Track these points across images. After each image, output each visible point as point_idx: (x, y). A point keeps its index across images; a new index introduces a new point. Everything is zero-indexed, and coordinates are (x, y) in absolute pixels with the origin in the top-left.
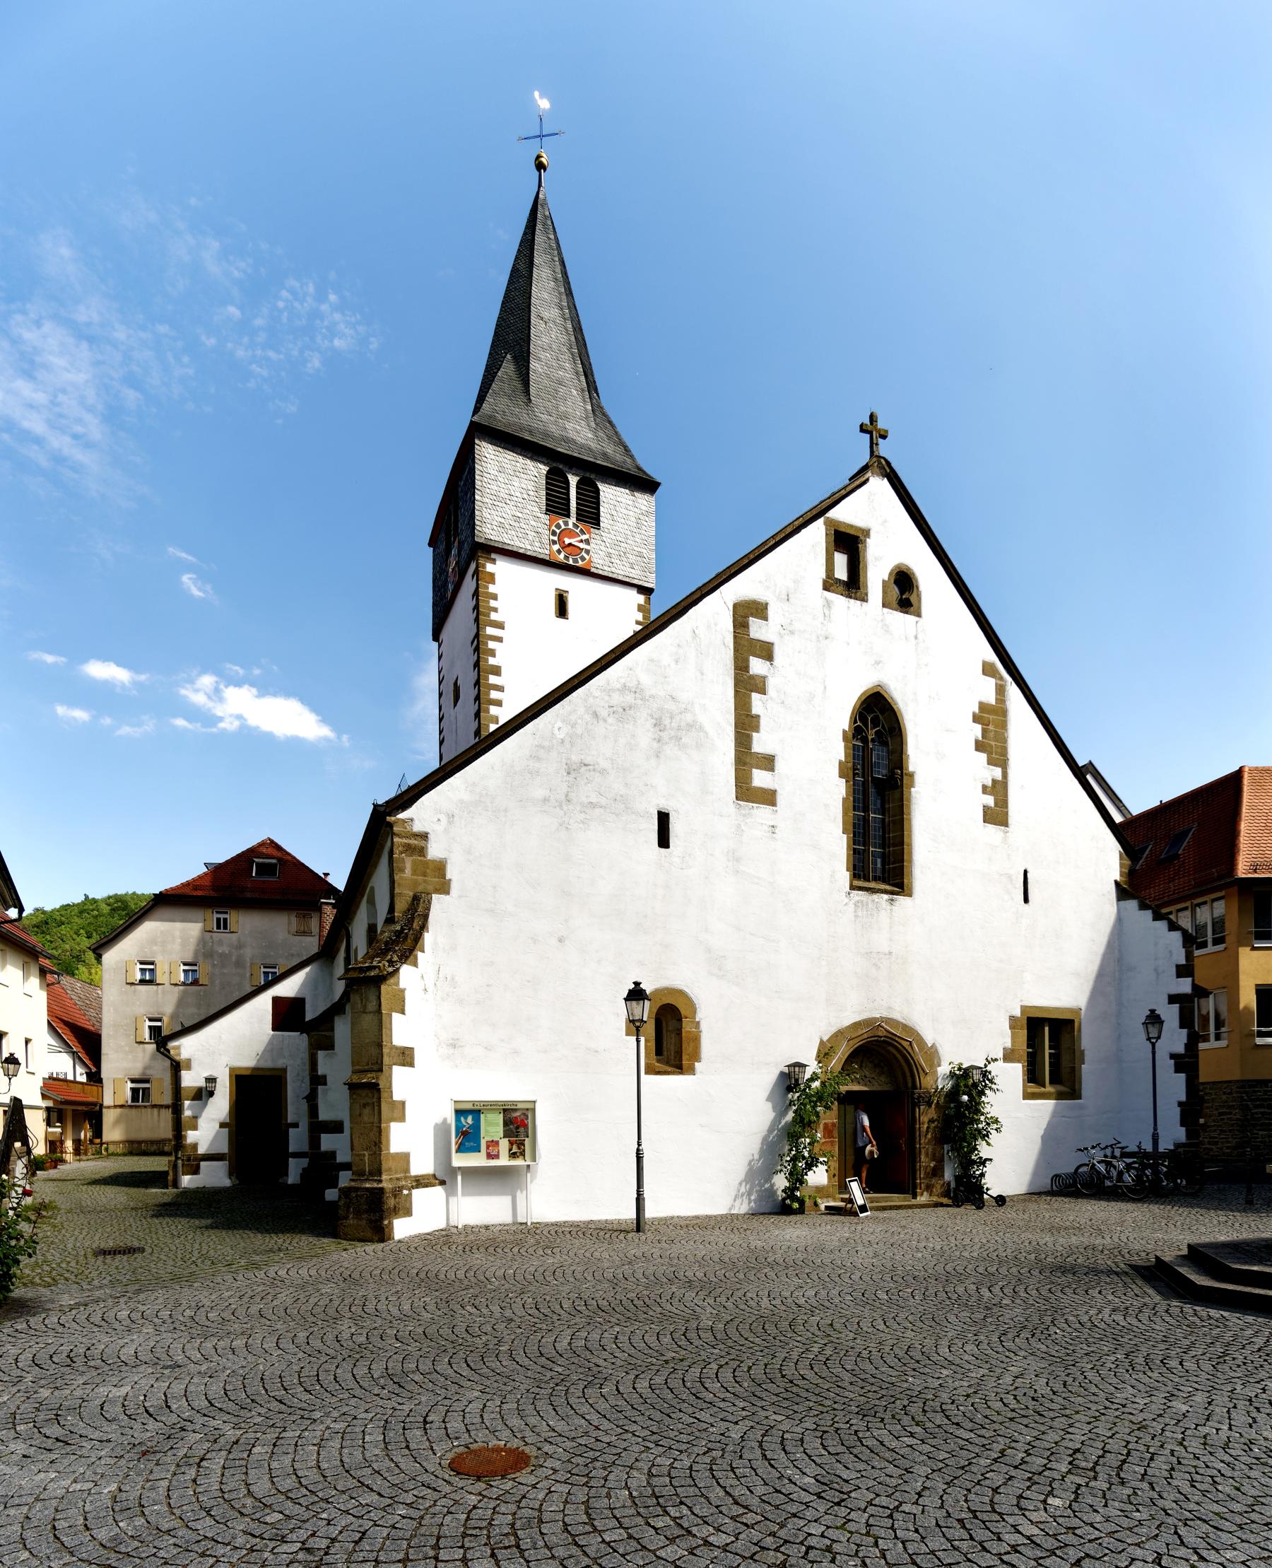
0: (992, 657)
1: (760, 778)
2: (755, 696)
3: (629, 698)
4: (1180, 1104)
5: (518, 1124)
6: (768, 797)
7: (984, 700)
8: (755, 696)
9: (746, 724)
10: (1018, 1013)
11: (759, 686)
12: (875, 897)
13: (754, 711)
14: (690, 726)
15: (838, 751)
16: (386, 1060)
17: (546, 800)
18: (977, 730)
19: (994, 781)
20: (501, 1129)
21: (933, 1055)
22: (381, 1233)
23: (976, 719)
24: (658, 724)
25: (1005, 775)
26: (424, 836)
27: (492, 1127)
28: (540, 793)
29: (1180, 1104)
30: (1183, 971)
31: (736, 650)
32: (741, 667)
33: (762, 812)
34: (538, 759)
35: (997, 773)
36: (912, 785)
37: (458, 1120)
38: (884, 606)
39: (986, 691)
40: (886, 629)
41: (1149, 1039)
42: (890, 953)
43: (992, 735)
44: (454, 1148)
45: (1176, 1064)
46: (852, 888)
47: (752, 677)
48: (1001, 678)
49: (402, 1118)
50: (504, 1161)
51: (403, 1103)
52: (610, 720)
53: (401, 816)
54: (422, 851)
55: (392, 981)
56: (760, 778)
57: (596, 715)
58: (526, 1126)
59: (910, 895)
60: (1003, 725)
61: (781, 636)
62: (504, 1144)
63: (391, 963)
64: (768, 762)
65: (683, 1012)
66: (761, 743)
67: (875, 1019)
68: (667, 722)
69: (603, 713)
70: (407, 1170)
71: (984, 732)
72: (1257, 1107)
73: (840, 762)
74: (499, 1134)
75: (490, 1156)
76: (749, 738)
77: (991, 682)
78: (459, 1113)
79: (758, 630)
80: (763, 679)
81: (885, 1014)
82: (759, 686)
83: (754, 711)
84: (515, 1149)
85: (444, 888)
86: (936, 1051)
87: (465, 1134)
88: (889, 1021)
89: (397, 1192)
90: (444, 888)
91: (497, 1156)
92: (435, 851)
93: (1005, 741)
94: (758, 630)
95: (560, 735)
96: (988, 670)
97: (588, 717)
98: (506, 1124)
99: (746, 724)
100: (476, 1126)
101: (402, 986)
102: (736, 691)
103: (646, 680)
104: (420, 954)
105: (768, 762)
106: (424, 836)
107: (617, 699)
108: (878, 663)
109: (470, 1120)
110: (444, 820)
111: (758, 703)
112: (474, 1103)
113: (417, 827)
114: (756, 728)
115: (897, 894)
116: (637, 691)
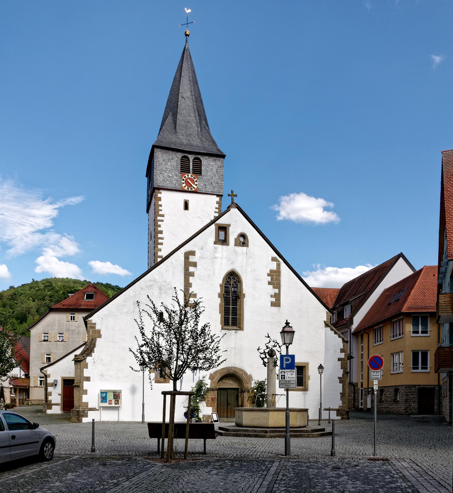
0: (275, 255)
2: (191, 278)
3: (152, 283)
4: (341, 393)
5: (117, 396)
7: (272, 269)
8: (191, 278)
9: (187, 285)
11: (192, 274)
12: (230, 331)
13: (190, 282)
15: (218, 290)
16: (82, 380)
17: (127, 312)
18: (269, 278)
19: (275, 294)
20: (113, 397)
21: (250, 378)
22: (80, 421)
23: (268, 275)
24: (160, 289)
25: (279, 291)
26: (95, 324)
27: (110, 397)
28: (126, 310)
29: (341, 393)
30: (342, 351)
31: (185, 265)
34: (126, 302)
35: (277, 291)
36: (244, 297)
37: (101, 395)
38: (235, 245)
39: (274, 266)
40: (236, 252)
41: (319, 373)
42: (235, 348)
43: (275, 279)
44: (100, 401)
46: (222, 329)
47: (190, 272)
48: (279, 261)
49: (86, 394)
50: (113, 405)
51: (87, 390)
52: (146, 289)
53: (89, 319)
54: (94, 327)
55: (84, 361)
57: (142, 289)
58: (119, 396)
59: (243, 330)
60: (279, 276)
61: (200, 260)
62: (113, 401)
63: (84, 357)
67: (230, 367)
68: (163, 288)
69: (144, 288)
70: (88, 406)
72: (411, 395)
74: (112, 398)
75: (109, 404)
76: (189, 290)
77: (275, 263)
78: (102, 393)
79: (192, 259)
80: (193, 273)
81: (233, 366)
82: (192, 274)
83: (190, 282)
84: (116, 402)
85: (100, 336)
86: (251, 376)
87: (103, 398)
88: (234, 368)
89: (83, 411)
90: (100, 336)
91: (111, 404)
92: (97, 328)
93: (280, 281)
94: (192, 259)
95: (132, 295)
96: (273, 259)
97: (140, 289)
98: (114, 396)
99: (187, 285)
100: (106, 396)
101: (87, 362)
102: (185, 277)
103: (157, 277)
104: (93, 353)
106: (95, 324)
107: (148, 284)
108: (232, 263)
109: (104, 395)
110: (100, 320)
111: (191, 279)
112: (105, 390)
113: (93, 322)
114: (191, 287)
115: (238, 330)
116: (155, 280)
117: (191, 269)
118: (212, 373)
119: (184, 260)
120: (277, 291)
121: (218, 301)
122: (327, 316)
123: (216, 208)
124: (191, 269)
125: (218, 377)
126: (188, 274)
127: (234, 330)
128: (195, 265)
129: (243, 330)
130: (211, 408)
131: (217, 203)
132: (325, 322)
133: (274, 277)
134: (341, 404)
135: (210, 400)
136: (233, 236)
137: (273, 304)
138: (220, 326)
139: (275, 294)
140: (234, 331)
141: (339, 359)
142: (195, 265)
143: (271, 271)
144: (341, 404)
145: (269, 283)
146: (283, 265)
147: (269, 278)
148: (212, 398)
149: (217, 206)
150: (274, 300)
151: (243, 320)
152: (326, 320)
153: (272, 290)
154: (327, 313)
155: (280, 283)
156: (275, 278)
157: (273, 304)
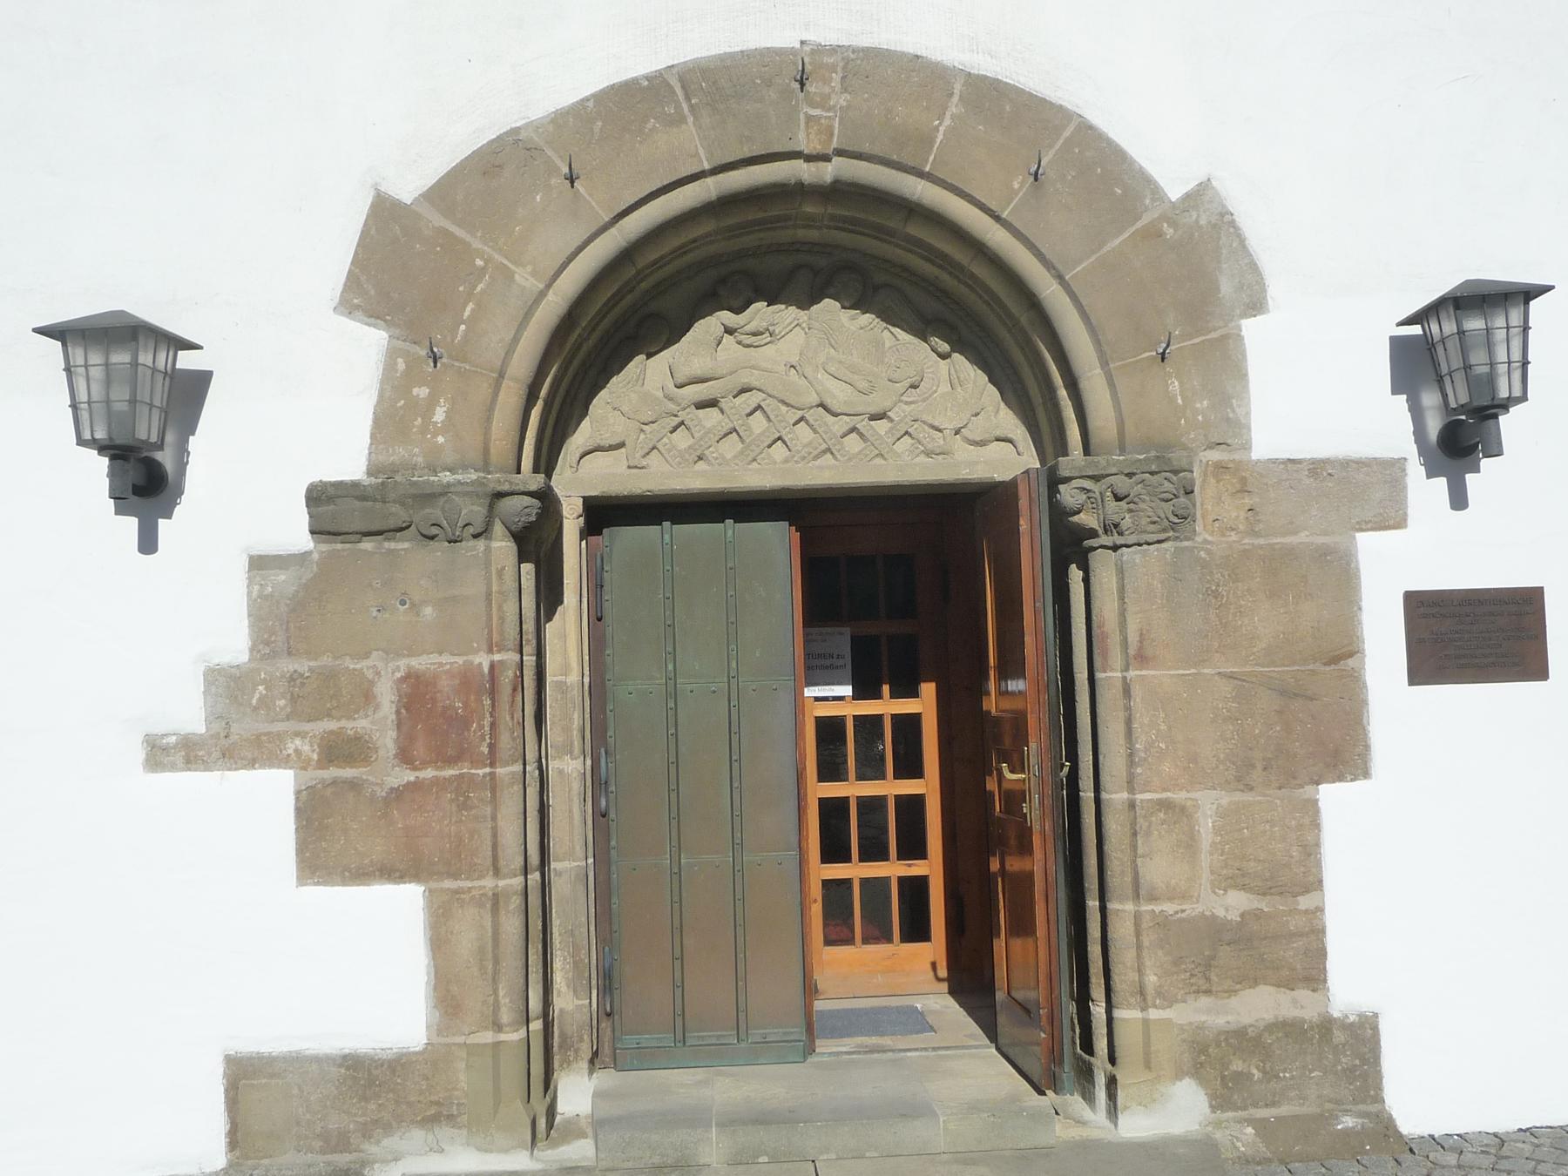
135: (380, 724)
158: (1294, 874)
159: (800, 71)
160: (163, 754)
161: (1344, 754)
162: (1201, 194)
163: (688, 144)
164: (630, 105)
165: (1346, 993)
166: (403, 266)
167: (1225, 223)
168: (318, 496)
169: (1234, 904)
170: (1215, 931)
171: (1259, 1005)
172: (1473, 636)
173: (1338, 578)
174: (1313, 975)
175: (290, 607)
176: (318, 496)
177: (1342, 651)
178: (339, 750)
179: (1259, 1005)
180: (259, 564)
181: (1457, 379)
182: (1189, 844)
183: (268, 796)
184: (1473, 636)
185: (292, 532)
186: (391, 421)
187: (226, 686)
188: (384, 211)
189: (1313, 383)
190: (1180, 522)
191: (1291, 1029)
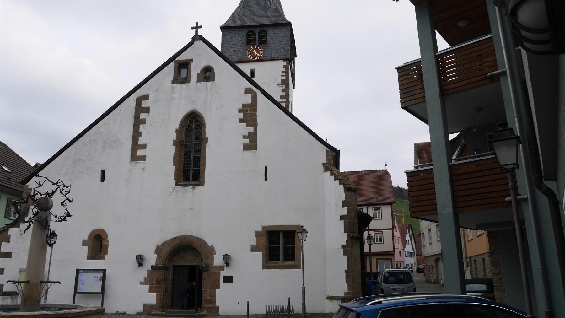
1: (140, 153)
6: (143, 158)
9: (137, 134)
10: (260, 229)
13: (140, 131)
14: (115, 141)
18: (241, 115)
23: (240, 111)
32: (137, 116)
33: (140, 164)
39: (248, 99)
45: (344, 251)
56: (140, 153)
60: (256, 110)
64: (144, 147)
65: (103, 237)
66: (141, 141)
71: (244, 116)
73: (174, 141)
76: (138, 140)
93: (256, 116)
96: (247, 91)
99: (137, 134)
105: (144, 147)
114: (141, 136)
117: (143, 116)
118: (159, 245)
119: (134, 106)
120: (251, 129)
121: (173, 150)
122: (327, 156)
123: (283, 72)
124: (143, 116)
125: (167, 249)
126: (138, 122)
127: (192, 185)
128: (147, 110)
129: (203, 185)
130: (155, 295)
131: (284, 66)
132: (324, 164)
133: (248, 112)
134: (347, 290)
135: (154, 282)
136: (195, 70)
137: (246, 147)
138: (173, 182)
139: (249, 133)
140: (191, 187)
141: (342, 218)
142: (147, 110)
143: (244, 106)
144: (347, 290)
145: (241, 121)
146: (260, 96)
147: (241, 115)
148: (157, 280)
149: (284, 70)
150: (247, 141)
151: (204, 171)
152: (325, 161)
153: (245, 129)
154: (327, 151)
155: (256, 119)
156: (249, 114)
157: (246, 147)
158: (214, 296)
159: (185, 237)
160: (141, 283)
161: (219, 288)
162: (212, 246)
163: (178, 242)
164: (174, 239)
165: (217, 304)
166: (158, 250)
167: (213, 248)
168: (152, 266)
169: (210, 298)
170: (208, 300)
171: (211, 305)
172: (228, 279)
173: (219, 274)
174: (215, 303)
175: (150, 273)
176: (152, 266)
177: (219, 280)
178: (152, 284)
179: (211, 305)
180: (148, 271)
181: (227, 259)
182: (207, 294)
183: (147, 287)
184: (228, 279)
185: (150, 269)
186: (156, 261)
187: (145, 279)
188: (158, 246)
189: (218, 260)
190: (208, 270)
191: (213, 307)
